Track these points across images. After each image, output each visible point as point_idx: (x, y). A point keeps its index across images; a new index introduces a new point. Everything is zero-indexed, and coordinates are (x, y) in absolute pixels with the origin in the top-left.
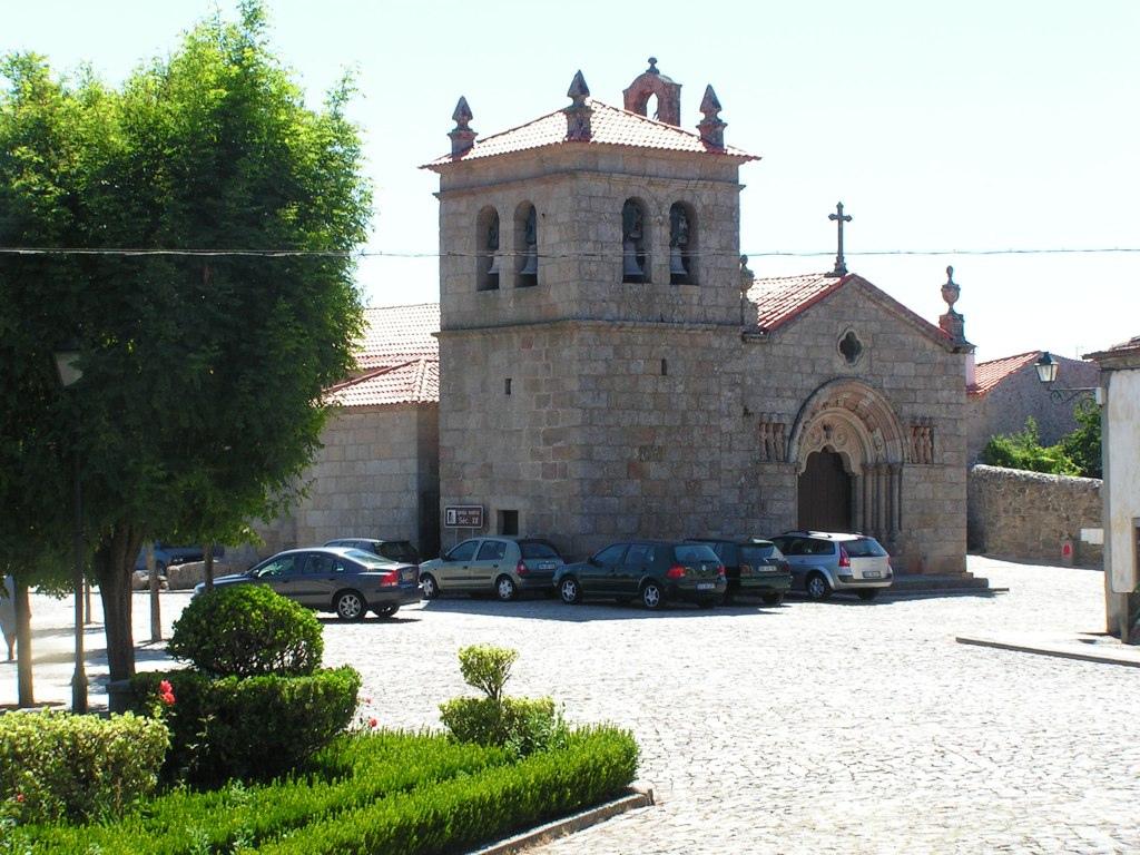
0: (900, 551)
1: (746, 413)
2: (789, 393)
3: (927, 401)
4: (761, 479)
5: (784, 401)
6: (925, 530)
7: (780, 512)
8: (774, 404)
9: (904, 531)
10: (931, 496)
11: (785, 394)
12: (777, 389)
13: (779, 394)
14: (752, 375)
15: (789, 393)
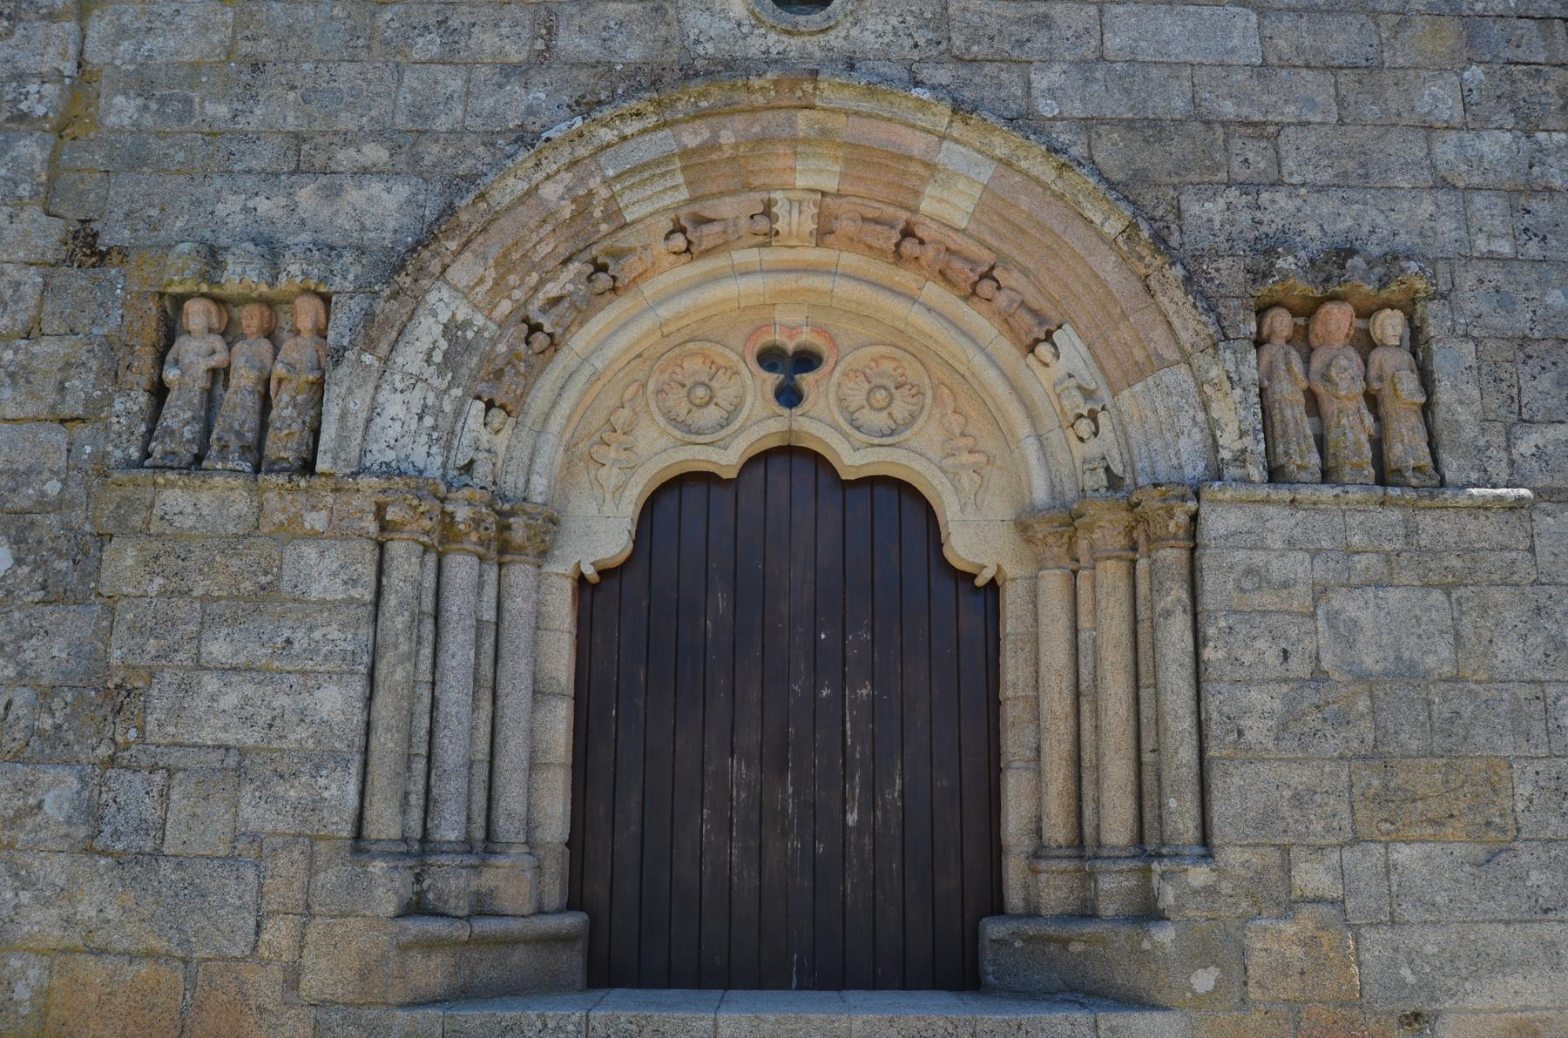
0: (1204, 980)
1: (87, 248)
2: (375, 153)
3: (1359, 179)
4: (123, 560)
5: (332, 193)
6: (1403, 854)
7: (251, 738)
8: (263, 205)
9: (1232, 856)
10: (1439, 658)
11: (346, 158)
12: (299, 138)
13: (303, 158)
14: (142, 84)
15: (375, 153)
